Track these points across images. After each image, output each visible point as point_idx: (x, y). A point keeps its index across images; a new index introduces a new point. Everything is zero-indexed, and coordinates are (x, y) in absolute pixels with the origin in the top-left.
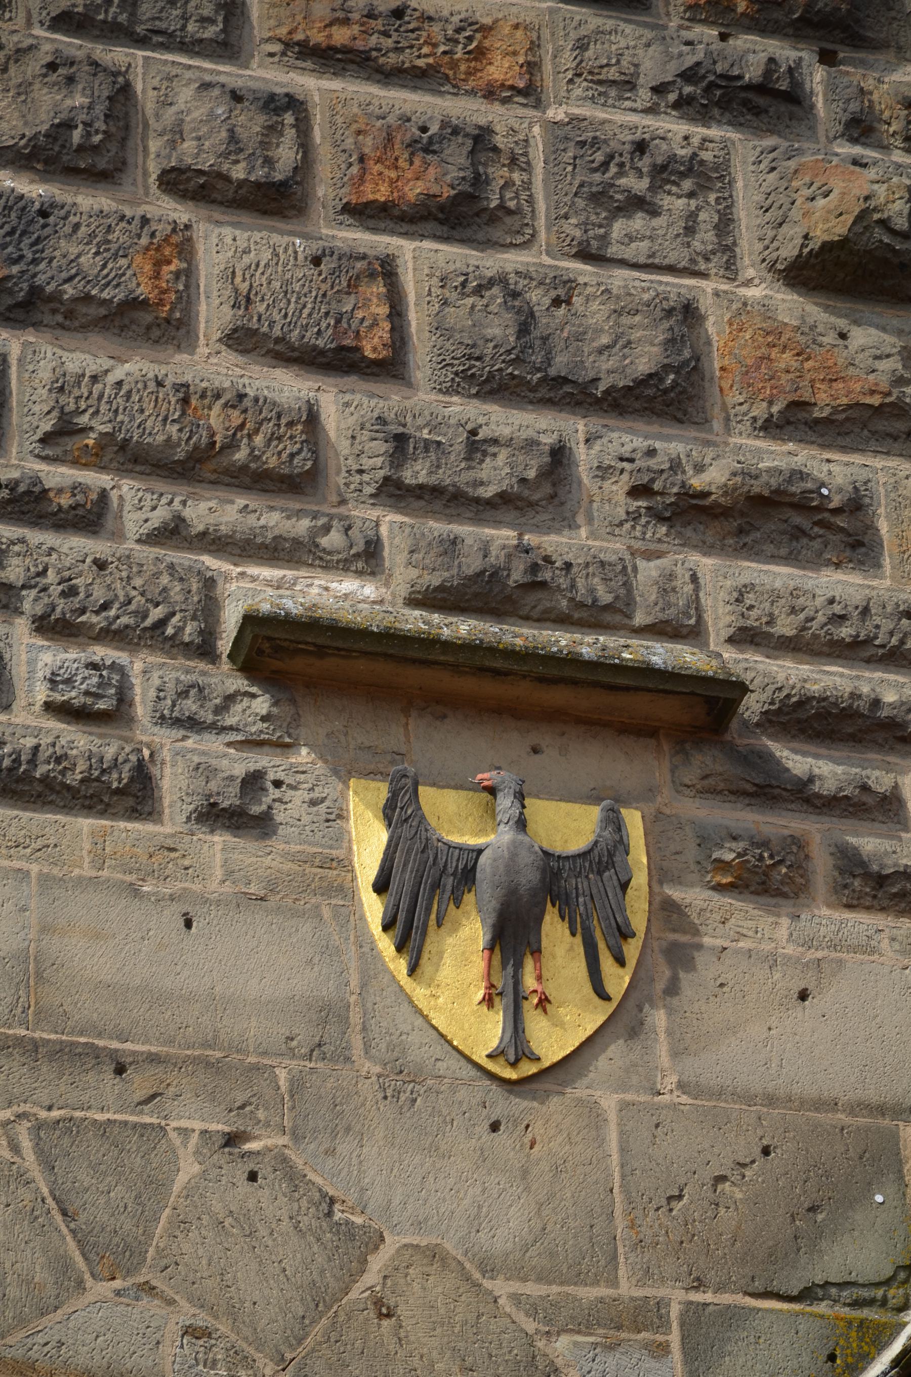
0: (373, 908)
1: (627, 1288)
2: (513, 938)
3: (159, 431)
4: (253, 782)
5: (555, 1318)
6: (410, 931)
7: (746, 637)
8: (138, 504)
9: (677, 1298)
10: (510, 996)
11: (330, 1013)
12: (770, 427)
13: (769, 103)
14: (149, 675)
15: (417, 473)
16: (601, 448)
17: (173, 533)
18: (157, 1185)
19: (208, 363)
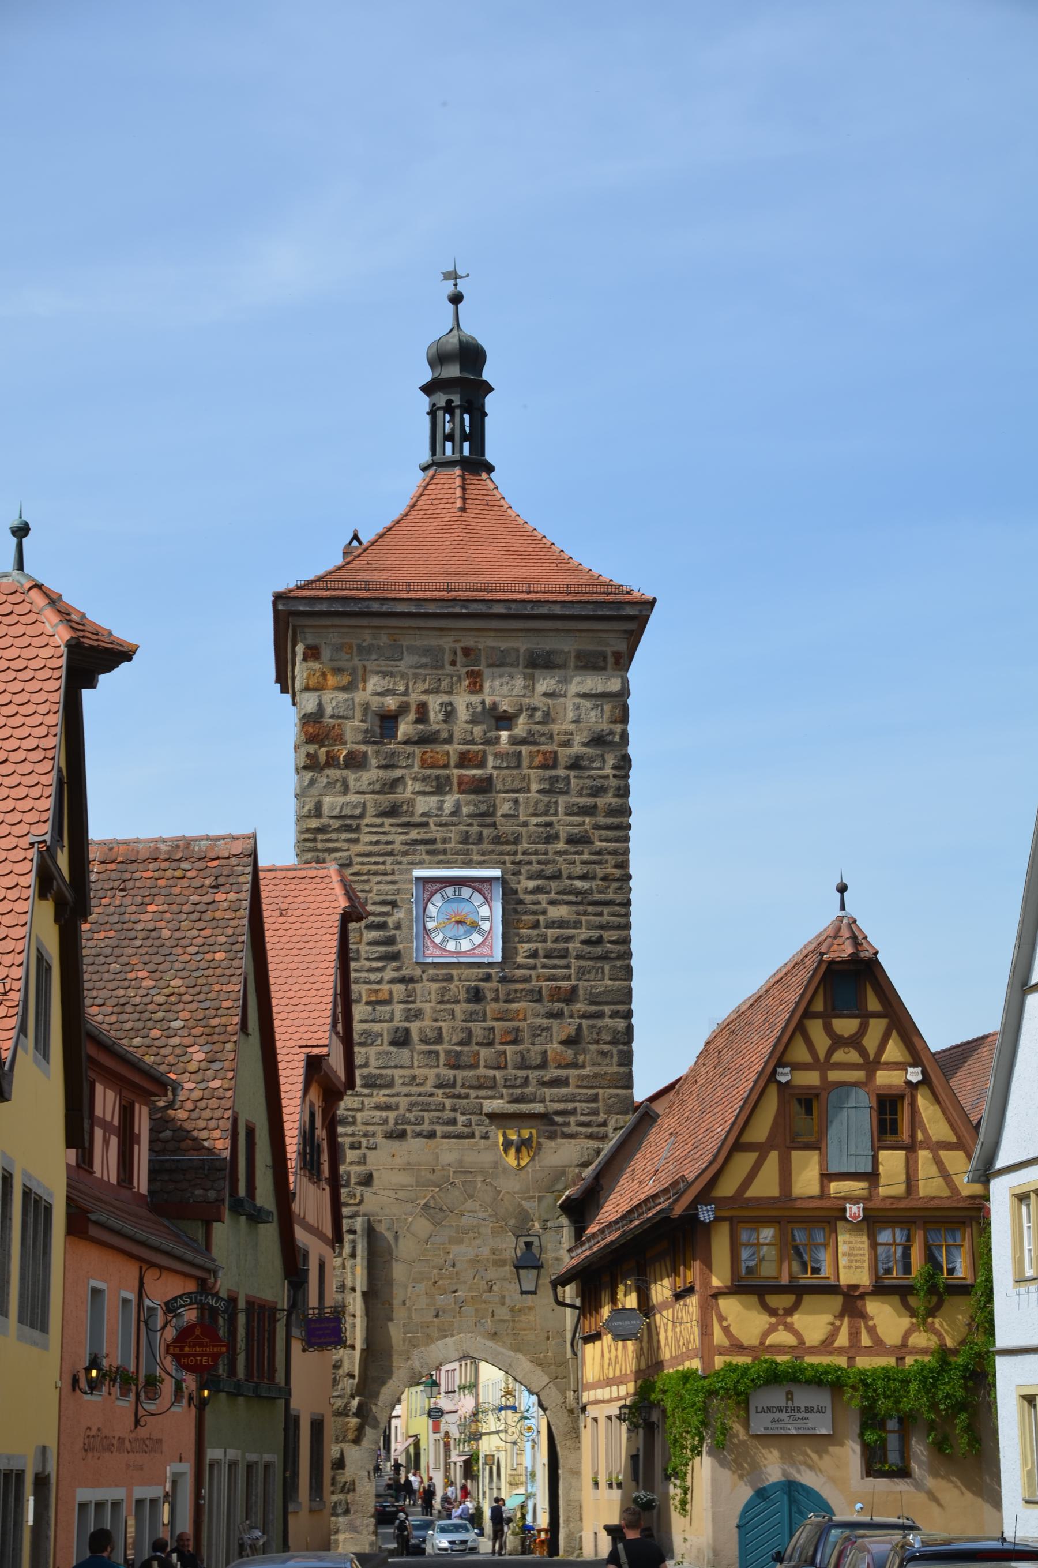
0: (501, 1148)
1: (531, 1194)
2: (518, 1151)
3: (475, 1083)
4: (487, 1132)
5: (522, 1199)
6: (506, 1151)
7: (551, 1101)
8: (473, 1093)
9: (537, 1194)
10: (518, 1158)
11: (496, 1163)
12: (556, 1068)
13: (558, 1015)
14: (474, 1118)
15: (508, 1084)
16: (533, 1075)
17: (477, 1097)
18: (475, 1187)
19: (482, 1071)
